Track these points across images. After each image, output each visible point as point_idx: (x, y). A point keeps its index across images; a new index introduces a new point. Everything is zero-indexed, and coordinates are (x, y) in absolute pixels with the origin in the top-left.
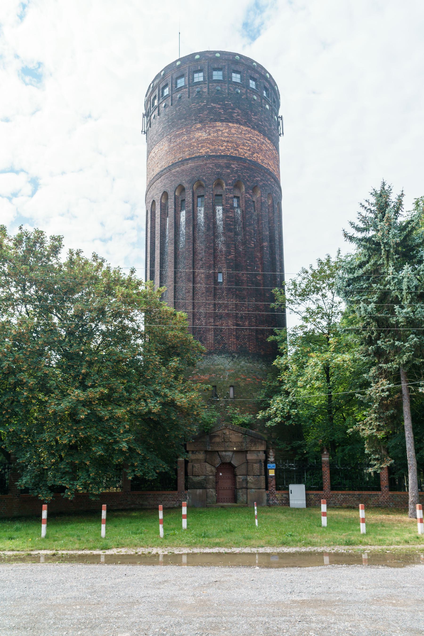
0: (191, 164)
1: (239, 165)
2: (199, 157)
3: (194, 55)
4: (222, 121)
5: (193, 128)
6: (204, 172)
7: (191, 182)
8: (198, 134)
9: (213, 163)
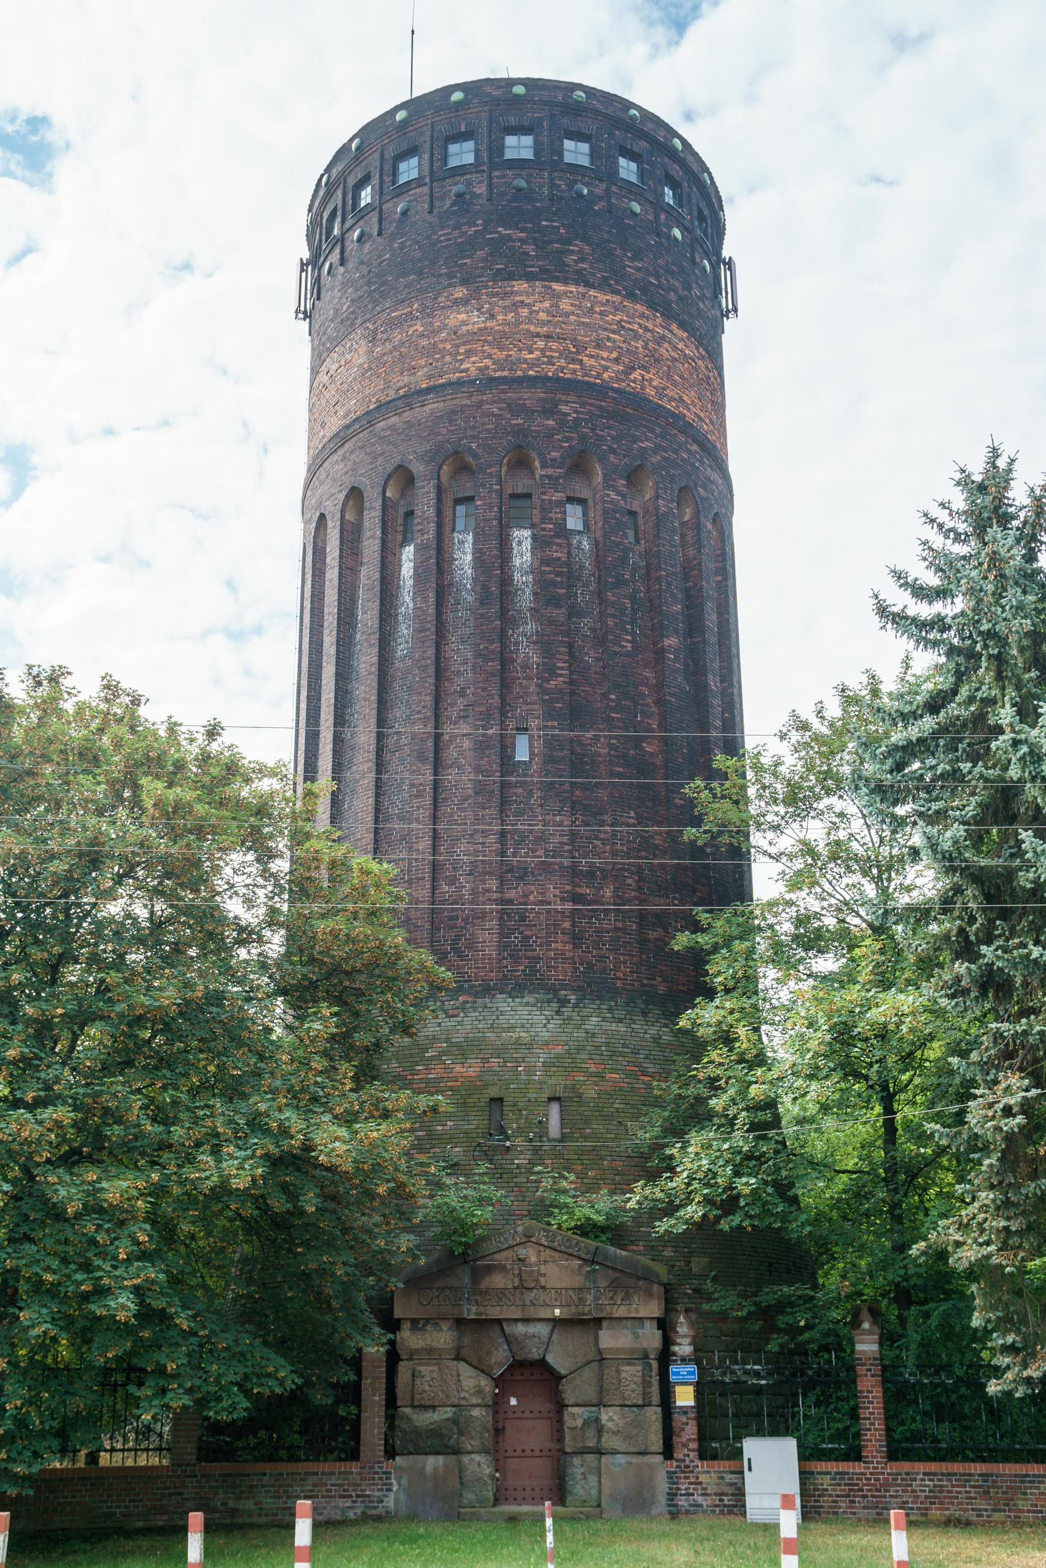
0: (434, 406)
1: (583, 405)
2: (460, 383)
3: (447, 91)
4: (530, 277)
6: (474, 428)
8: (456, 317)
9: (503, 401)
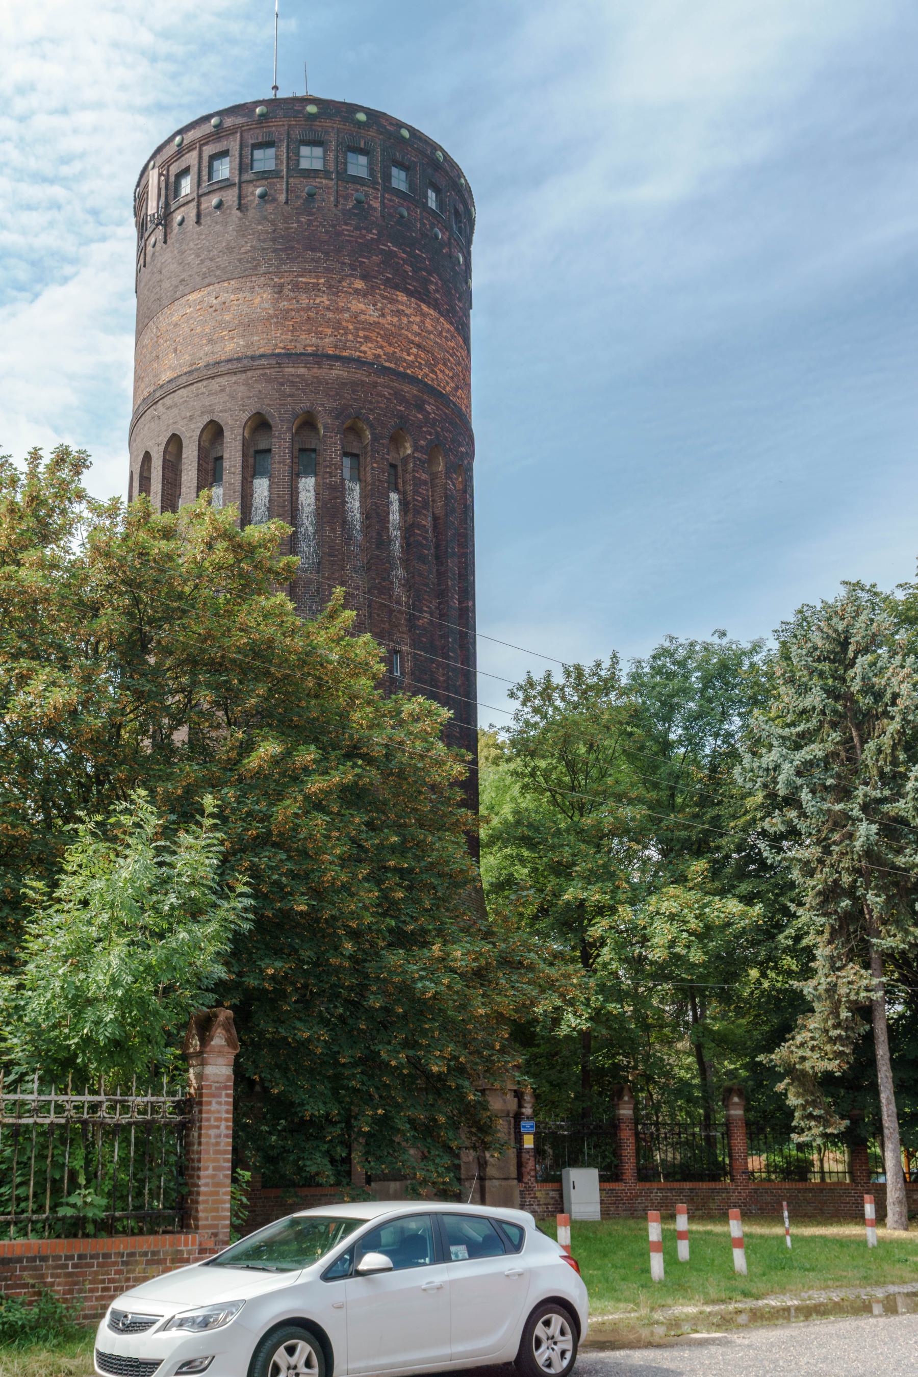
0: (338, 372)
1: (438, 408)
2: (358, 361)
3: (353, 108)
4: (410, 294)
5: (344, 284)
6: (370, 402)
7: (339, 414)
8: (357, 305)
9: (391, 388)
